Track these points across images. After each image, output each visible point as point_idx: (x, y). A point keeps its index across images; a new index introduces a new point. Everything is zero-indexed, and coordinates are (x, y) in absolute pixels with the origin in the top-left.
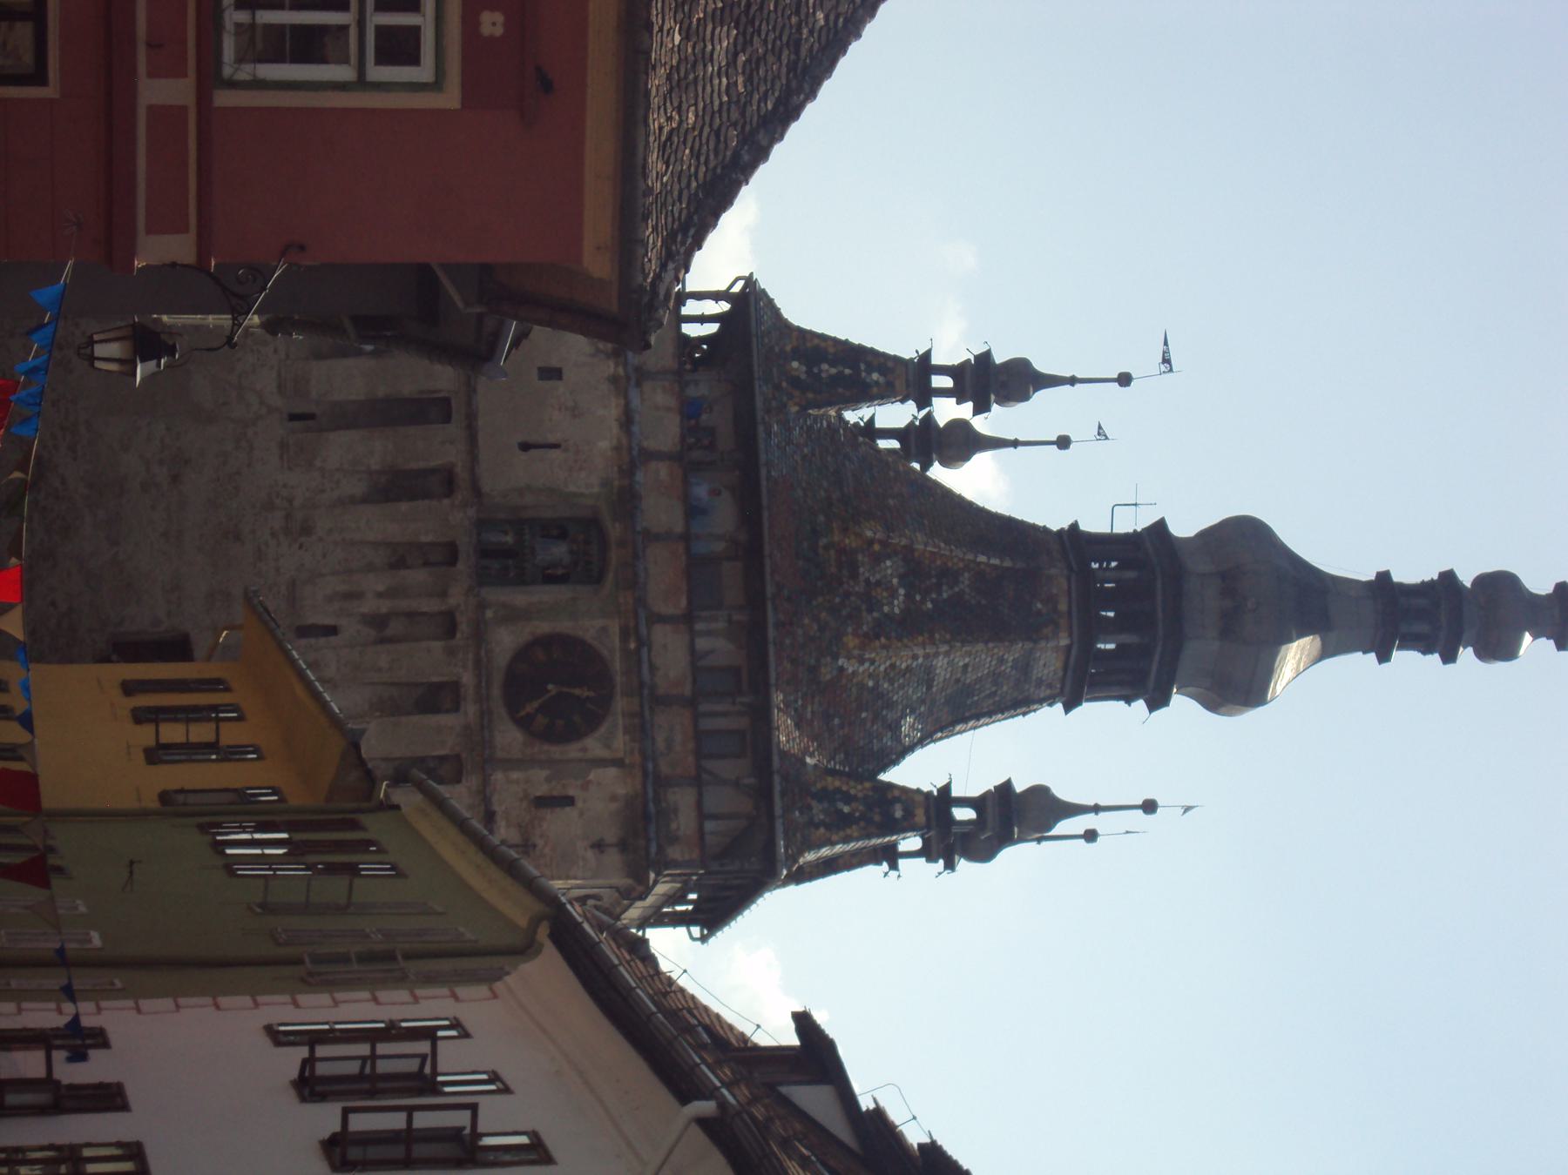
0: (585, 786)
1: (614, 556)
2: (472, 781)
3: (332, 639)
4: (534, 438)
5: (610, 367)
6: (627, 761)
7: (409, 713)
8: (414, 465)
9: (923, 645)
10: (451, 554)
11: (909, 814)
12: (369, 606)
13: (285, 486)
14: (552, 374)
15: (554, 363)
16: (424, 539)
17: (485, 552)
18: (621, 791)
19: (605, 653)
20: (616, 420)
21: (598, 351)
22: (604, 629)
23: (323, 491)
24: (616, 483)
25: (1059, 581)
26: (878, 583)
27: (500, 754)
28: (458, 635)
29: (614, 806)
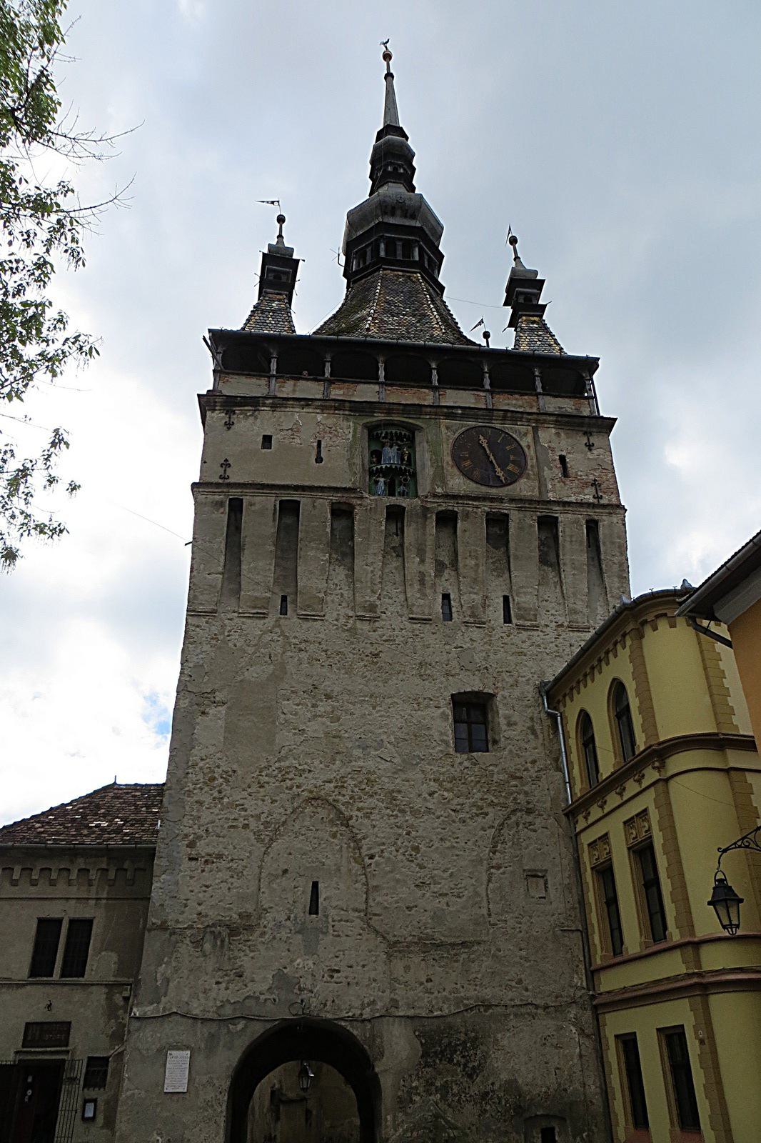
1: (396, 418)
3: (452, 597)
4: (314, 457)
6: (534, 425)
7: (508, 550)
8: (329, 530)
9: (432, 312)
10: (395, 515)
12: (429, 568)
13: (337, 620)
14: (267, 440)
15: (260, 439)
16: (383, 528)
17: (392, 494)
18: (553, 430)
20: (303, 409)
22: (447, 428)
23: (342, 595)
24: (347, 413)
26: (399, 324)
27: (536, 492)
28: (456, 509)
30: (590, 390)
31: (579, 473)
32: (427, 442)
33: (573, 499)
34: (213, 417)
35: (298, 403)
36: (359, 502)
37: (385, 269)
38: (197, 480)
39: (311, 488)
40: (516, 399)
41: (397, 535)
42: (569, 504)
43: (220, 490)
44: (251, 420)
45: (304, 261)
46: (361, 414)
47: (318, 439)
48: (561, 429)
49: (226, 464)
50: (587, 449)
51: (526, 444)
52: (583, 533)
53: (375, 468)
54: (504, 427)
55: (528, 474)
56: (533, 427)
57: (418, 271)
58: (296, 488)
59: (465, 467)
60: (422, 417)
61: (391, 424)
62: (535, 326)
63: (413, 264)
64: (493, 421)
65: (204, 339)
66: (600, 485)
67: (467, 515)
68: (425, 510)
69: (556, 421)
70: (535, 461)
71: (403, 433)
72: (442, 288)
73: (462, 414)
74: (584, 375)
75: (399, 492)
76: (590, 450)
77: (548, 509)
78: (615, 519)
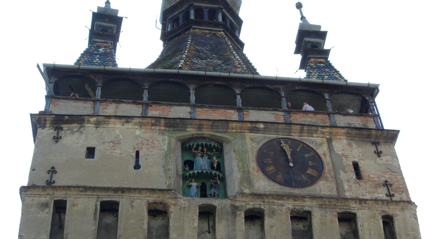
0: (347, 157)
1: (206, 132)
2: (354, 207)
4: (133, 163)
5: (90, 127)
6: (328, 137)
8: (145, 227)
9: (235, 57)
11: (321, 63)
16: (196, 225)
18: (345, 141)
19: (266, 140)
20: (123, 125)
21: (76, 131)
22: (252, 140)
24: (162, 128)
25: (197, 30)
28: (262, 207)
29: (354, 145)
30: (374, 109)
31: (372, 176)
32: (234, 151)
33: (368, 197)
34: (43, 133)
35: (119, 121)
36: (173, 202)
37: (194, 29)
38: (26, 184)
39: (129, 190)
40: (311, 117)
41: (209, 232)
42: (365, 200)
43: (46, 193)
44: (77, 135)
45: (127, 18)
46: (175, 129)
47: (136, 149)
48: (352, 140)
49: (53, 171)
50: (376, 156)
51: (323, 152)
52: (380, 227)
53: (188, 174)
54: (301, 138)
55: (326, 177)
56: (327, 139)
57: (222, 30)
58: (116, 190)
59: (270, 172)
60: (229, 131)
61: (203, 138)
62: (322, 65)
63: (217, 25)
64: (292, 134)
65: (38, 66)
66: (391, 185)
67: (273, 213)
68: (235, 209)
69: (348, 133)
70: (331, 166)
71: (213, 144)
72: (242, 45)
73: (265, 128)
74: (367, 98)
75: (211, 195)
76: (379, 156)
77: (347, 206)
78: (407, 214)
